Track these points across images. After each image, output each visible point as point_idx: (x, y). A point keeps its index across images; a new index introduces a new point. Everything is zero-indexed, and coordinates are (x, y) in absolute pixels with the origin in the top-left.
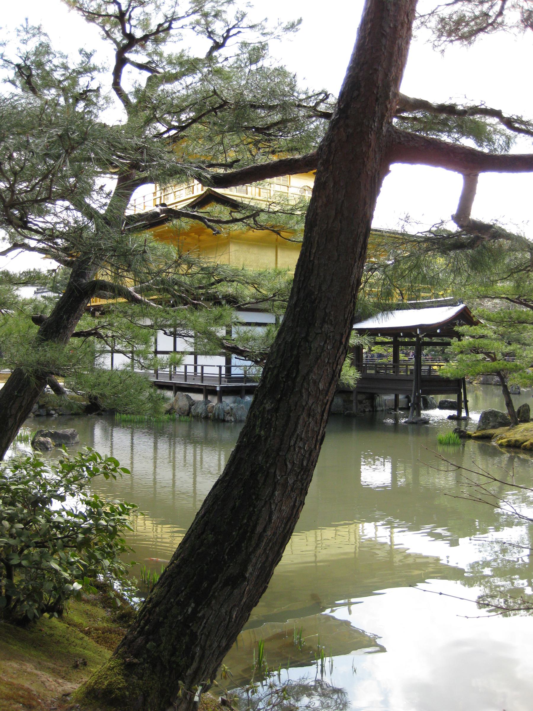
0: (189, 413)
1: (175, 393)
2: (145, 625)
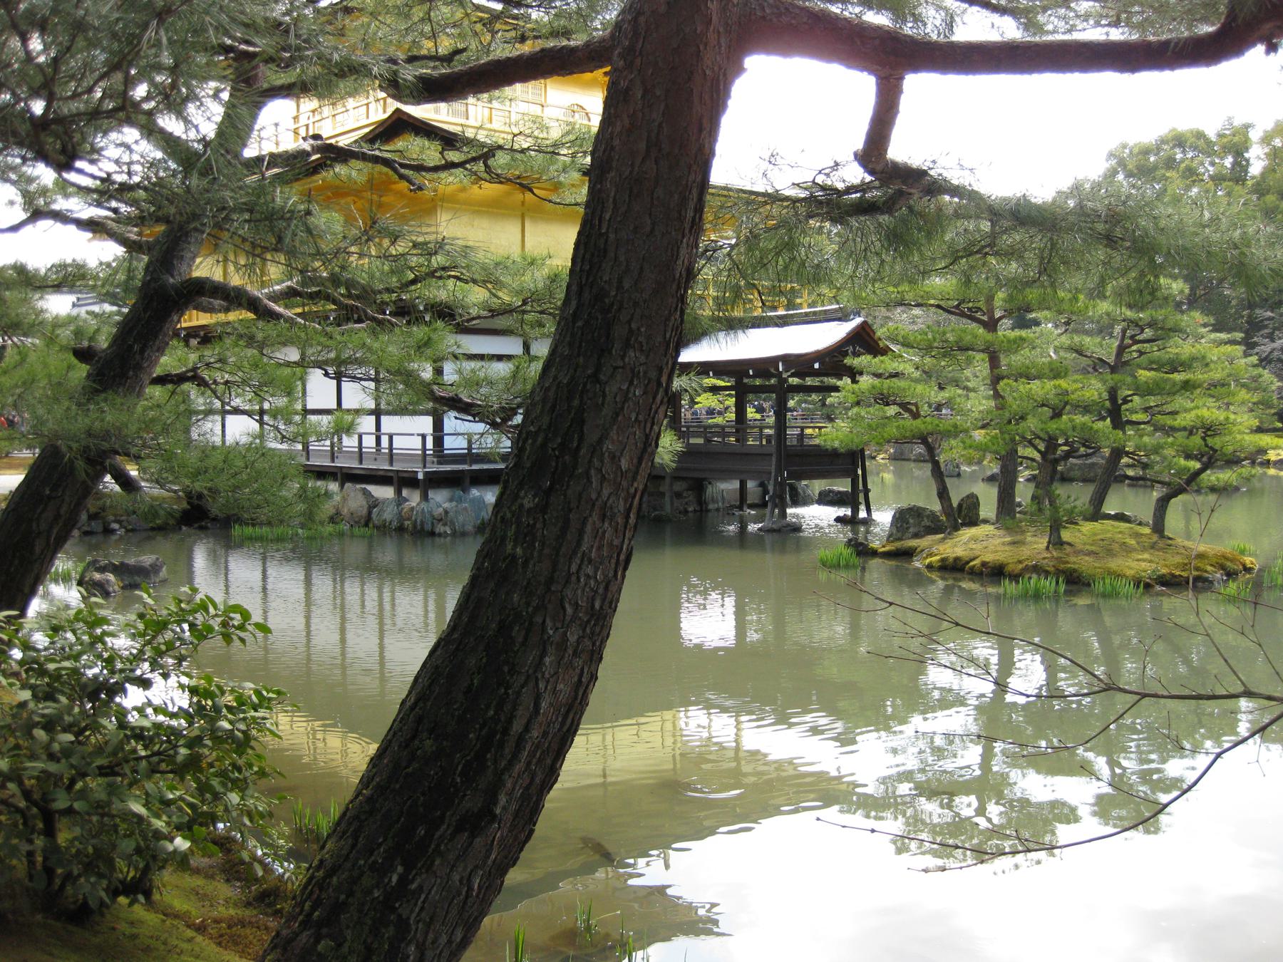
1: (342, 486)
2: (313, 909)
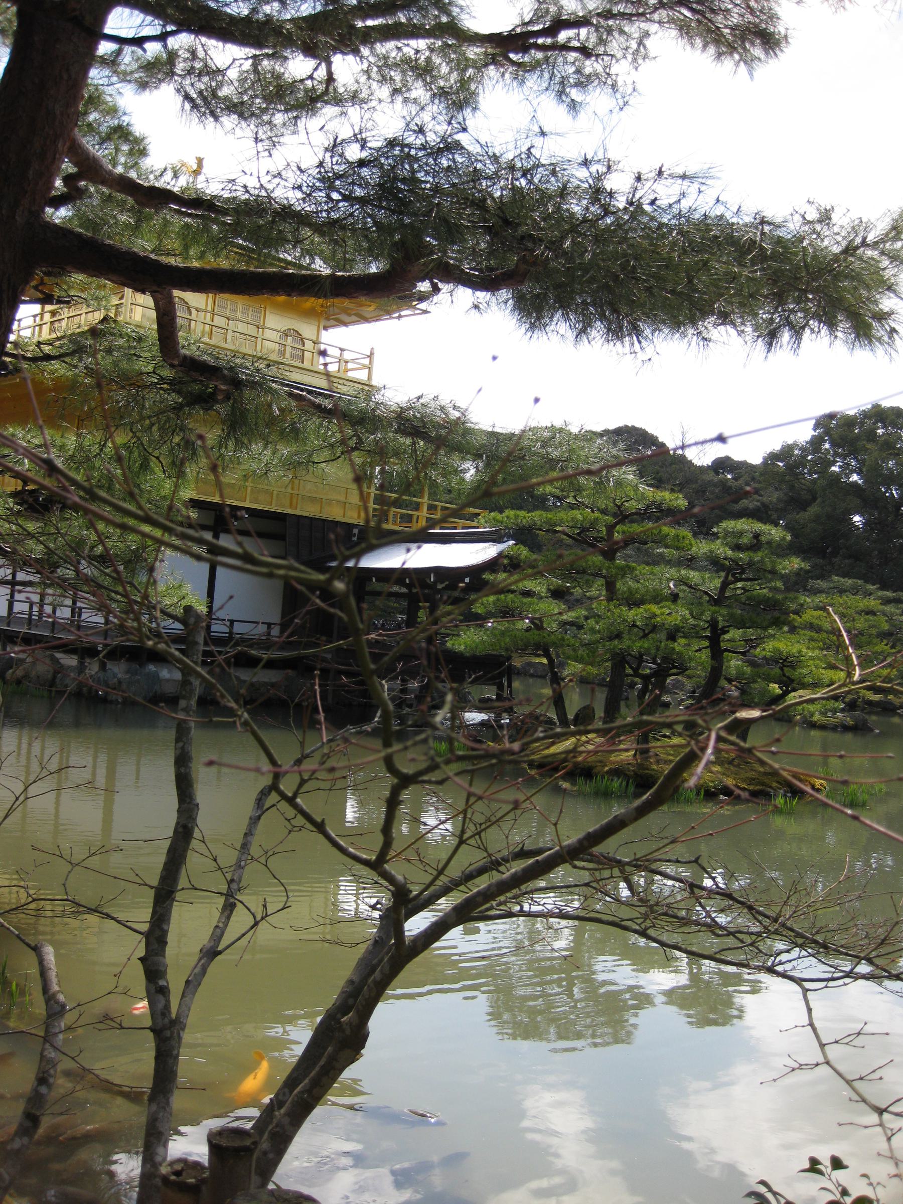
0: (52, 683)
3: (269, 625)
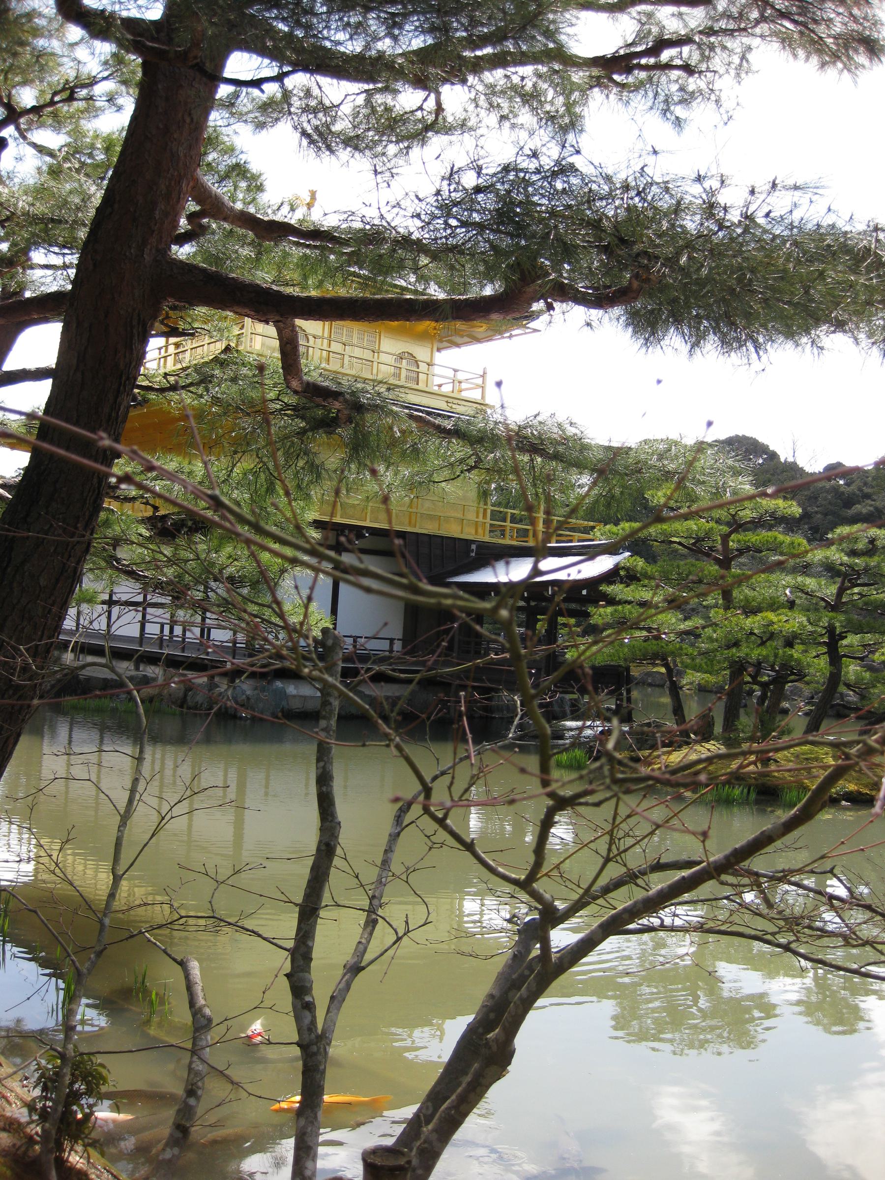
3: (392, 641)
